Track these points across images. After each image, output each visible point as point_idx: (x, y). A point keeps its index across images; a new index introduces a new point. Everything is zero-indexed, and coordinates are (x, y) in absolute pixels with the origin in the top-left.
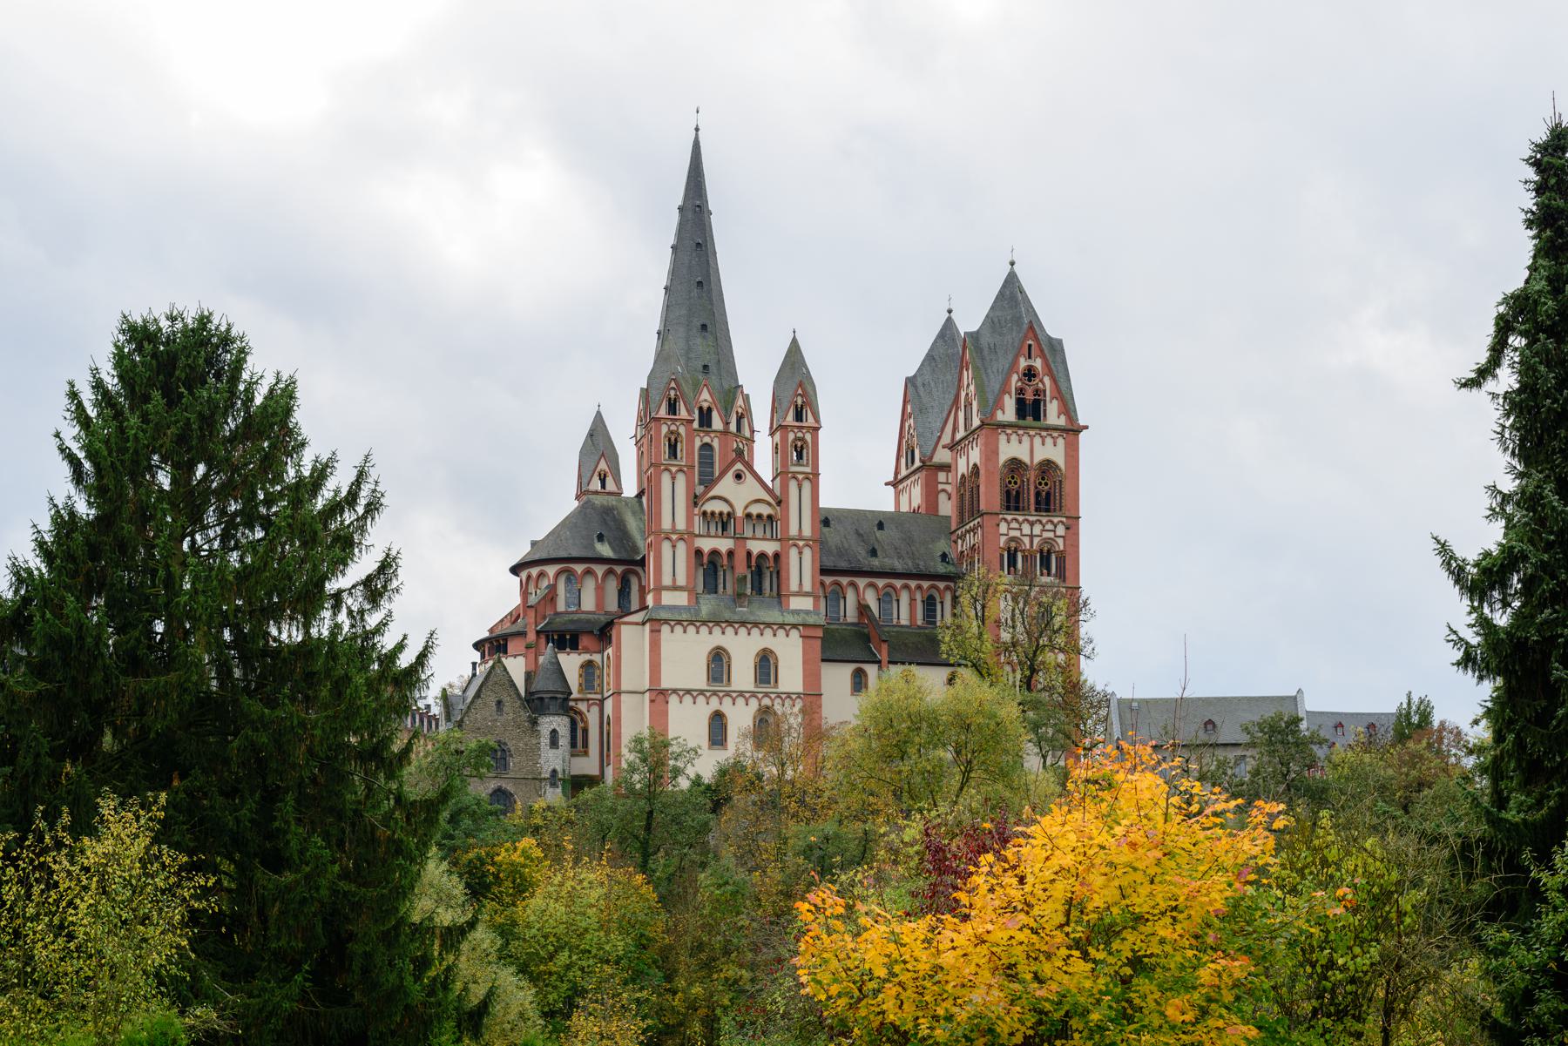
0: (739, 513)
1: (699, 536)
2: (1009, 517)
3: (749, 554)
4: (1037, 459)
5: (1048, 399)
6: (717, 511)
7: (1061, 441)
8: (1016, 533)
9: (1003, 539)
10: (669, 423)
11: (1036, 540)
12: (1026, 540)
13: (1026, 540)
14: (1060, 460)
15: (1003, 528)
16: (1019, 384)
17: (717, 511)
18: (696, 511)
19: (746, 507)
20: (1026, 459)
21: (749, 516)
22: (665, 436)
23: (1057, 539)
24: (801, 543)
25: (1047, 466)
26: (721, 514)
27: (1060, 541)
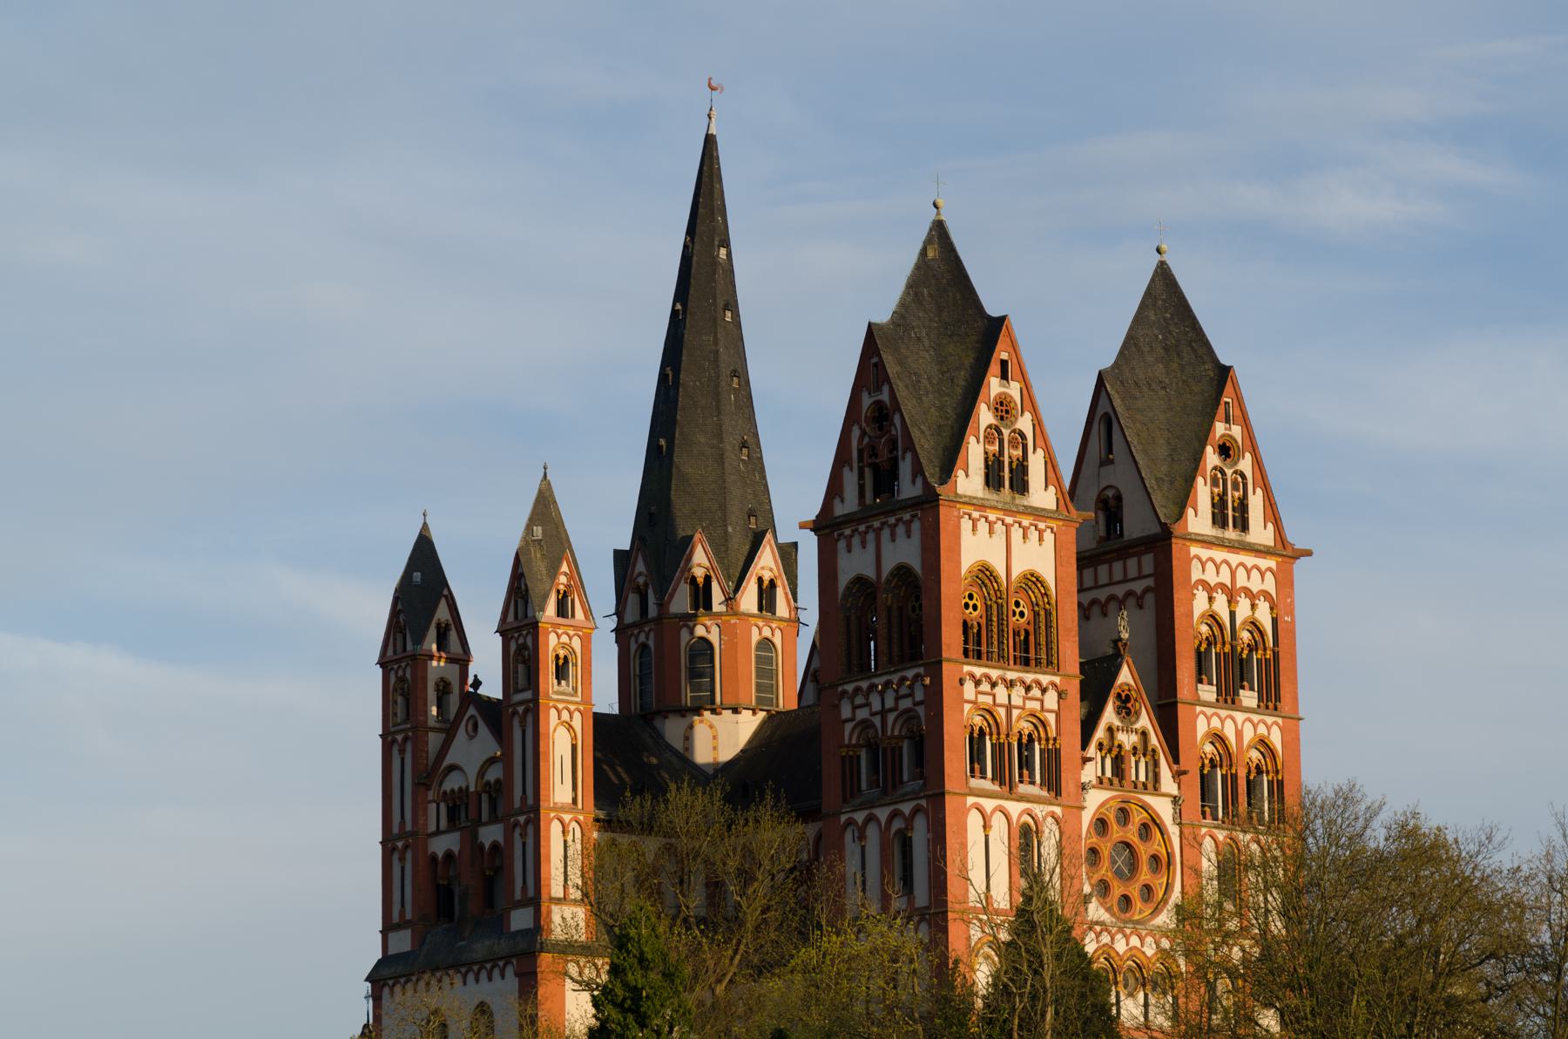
0: (472, 789)
1: (438, 832)
2: (850, 688)
3: (434, 858)
4: (887, 567)
5: (900, 453)
6: (456, 789)
7: (916, 526)
8: (862, 714)
9: (848, 727)
10: (395, 667)
11: (891, 717)
12: (877, 721)
13: (877, 721)
14: (916, 564)
15: (846, 711)
16: (866, 440)
17: (456, 789)
18: (431, 796)
19: (482, 773)
20: (871, 573)
21: (488, 783)
22: (395, 690)
23: (917, 708)
24: (522, 819)
25: (903, 571)
26: (460, 789)
27: (921, 710)
